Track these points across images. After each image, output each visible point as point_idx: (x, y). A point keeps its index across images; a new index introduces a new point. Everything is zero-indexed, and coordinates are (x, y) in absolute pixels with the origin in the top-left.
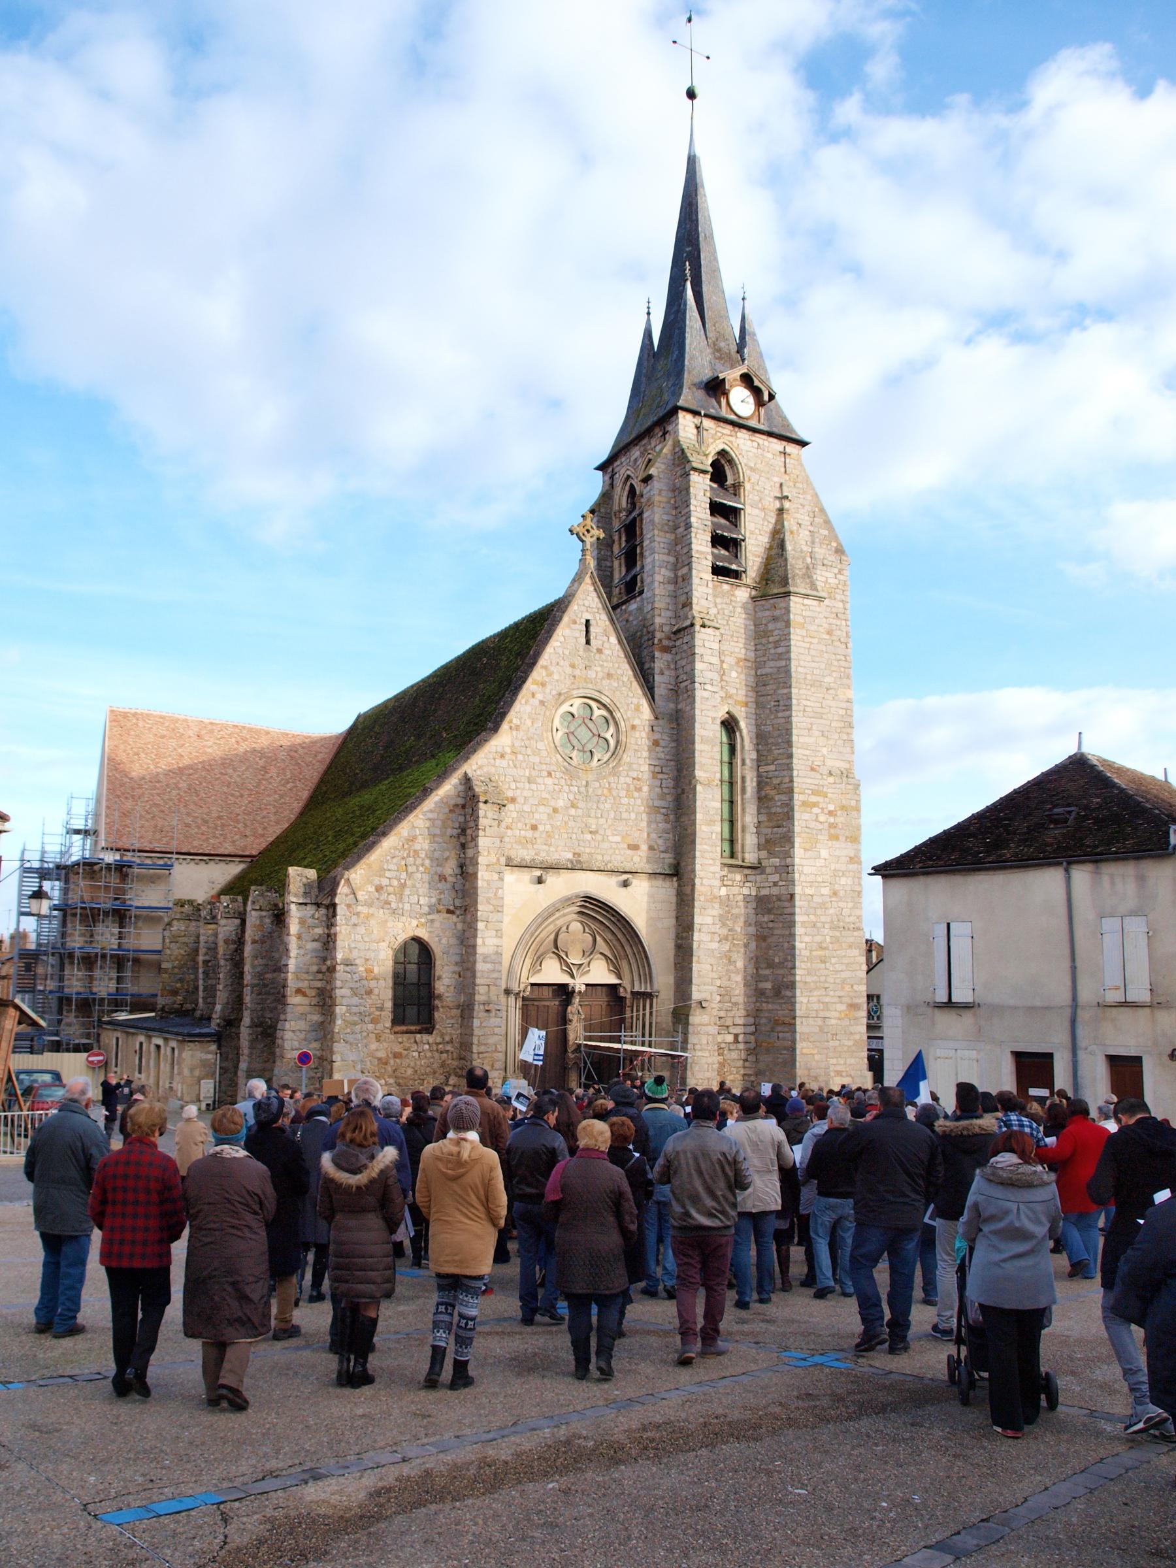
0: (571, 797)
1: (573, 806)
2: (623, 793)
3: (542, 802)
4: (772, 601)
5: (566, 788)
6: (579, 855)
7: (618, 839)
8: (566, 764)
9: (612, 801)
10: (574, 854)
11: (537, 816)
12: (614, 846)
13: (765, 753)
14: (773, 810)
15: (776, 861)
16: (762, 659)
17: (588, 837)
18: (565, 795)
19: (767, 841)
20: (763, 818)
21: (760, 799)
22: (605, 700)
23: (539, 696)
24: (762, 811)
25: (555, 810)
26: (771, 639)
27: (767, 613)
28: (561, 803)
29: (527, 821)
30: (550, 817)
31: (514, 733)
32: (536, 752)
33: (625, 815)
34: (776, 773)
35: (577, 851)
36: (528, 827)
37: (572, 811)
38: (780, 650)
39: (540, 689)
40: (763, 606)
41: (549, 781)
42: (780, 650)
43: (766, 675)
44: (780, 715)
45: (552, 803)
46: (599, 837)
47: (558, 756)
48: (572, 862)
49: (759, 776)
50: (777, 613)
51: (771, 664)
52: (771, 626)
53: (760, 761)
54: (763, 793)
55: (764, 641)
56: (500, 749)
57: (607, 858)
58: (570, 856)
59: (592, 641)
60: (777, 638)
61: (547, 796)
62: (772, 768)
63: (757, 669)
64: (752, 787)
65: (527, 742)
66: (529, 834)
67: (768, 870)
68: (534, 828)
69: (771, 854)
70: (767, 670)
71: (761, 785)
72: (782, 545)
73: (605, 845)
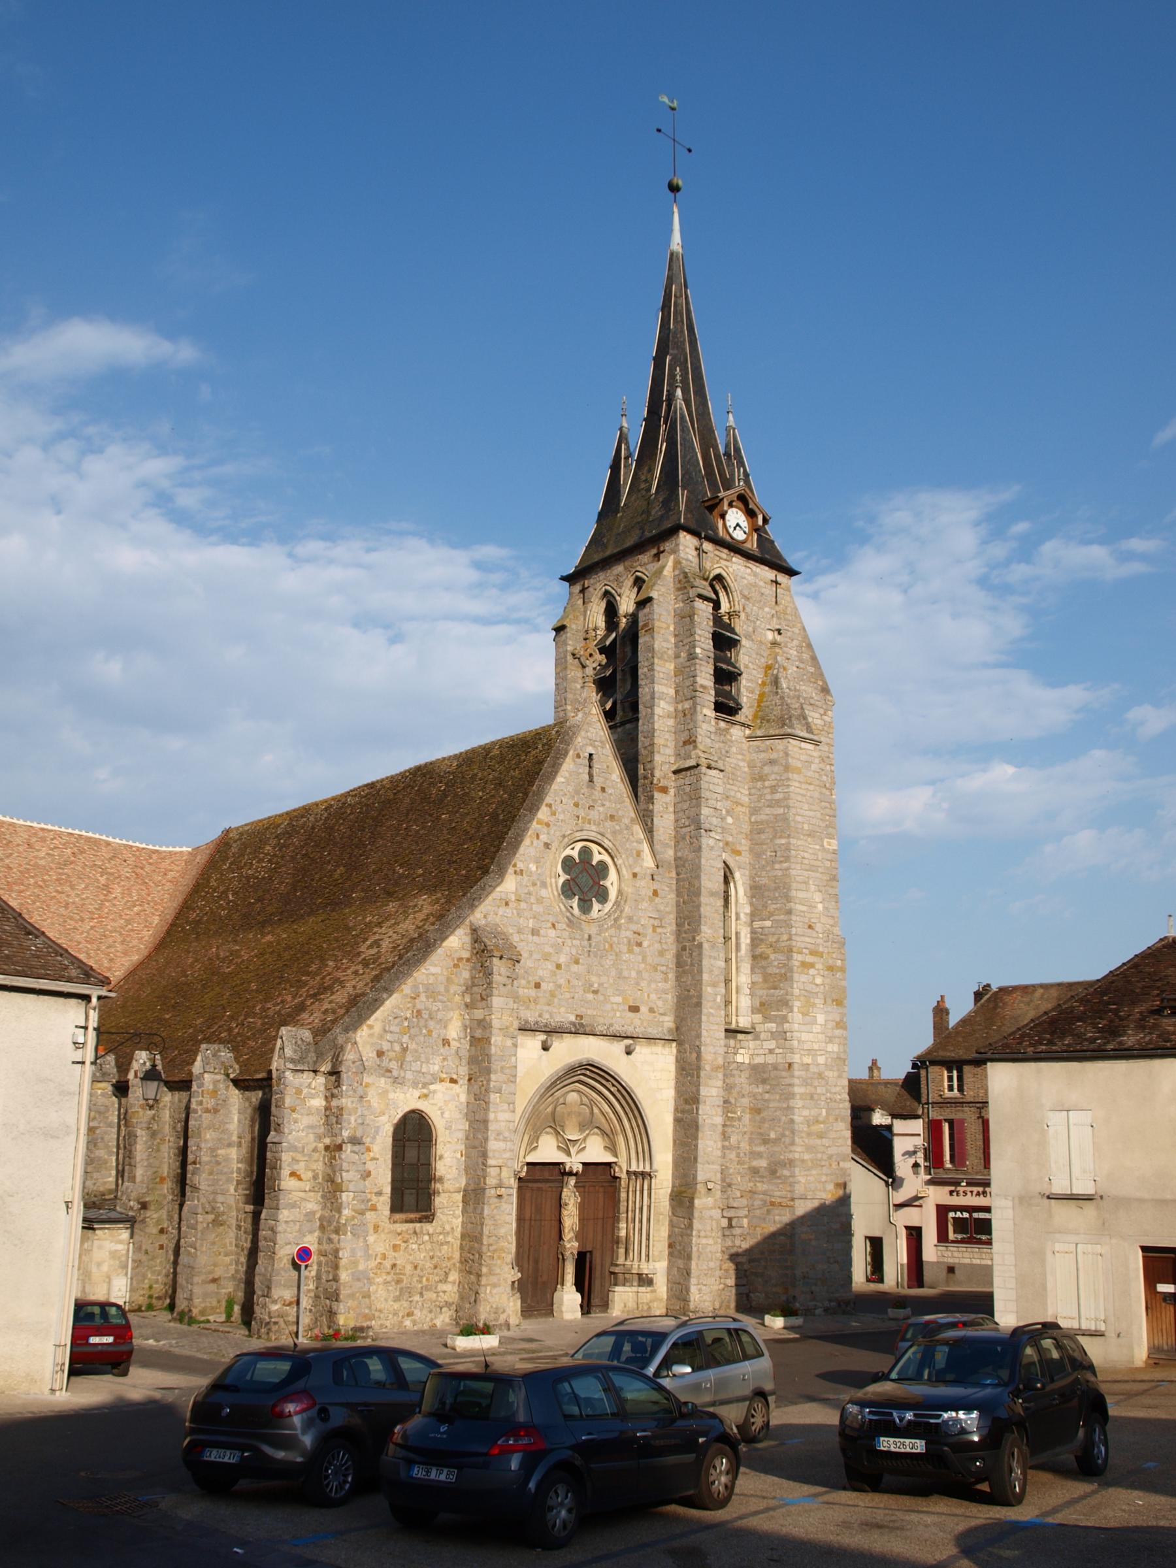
0: (574, 951)
1: (577, 962)
2: (624, 948)
3: (546, 957)
4: (768, 743)
5: (569, 942)
6: (581, 1017)
7: (619, 999)
8: (568, 914)
9: (614, 957)
10: (577, 1016)
11: (540, 973)
12: (615, 1007)
13: (760, 908)
14: (769, 970)
15: (772, 1026)
16: (756, 804)
17: (590, 996)
18: (568, 949)
19: (762, 1004)
20: (758, 978)
21: (754, 957)
22: (607, 843)
23: (544, 838)
24: (756, 970)
25: (558, 966)
26: (767, 784)
27: (763, 755)
28: (562, 959)
29: (530, 979)
30: (554, 974)
31: (519, 877)
32: (540, 900)
33: (625, 973)
34: (773, 930)
36: (533, 985)
37: (575, 968)
38: (778, 796)
39: (545, 830)
40: (758, 747)
41: (552, 933)
42: (778, 796)
43: (762, 823)
44: (777, 866)
45: (554, 959)
46: (601, 998)
47: (561, 905)
48: (574, 1024)
49: (753, 932)
50: (774, 756)
51: (768, 811)
52: (767, 769)
53: (754, 915)
54: (759, 951)
55: (759, 784)
56: (503, 896)
58: (572, 1018)
59: (595, 779)
60: (774, 783)
61: (551, 950)
62: (768, 923)
63: (752, 814)
64: (747, 944)
65: (531, 889)
66: (532, 992)
67: (763, 1036)
68: (538, 986)
69: (767, 1019)
70: (764, 817)
71: (755, 941)
72: (776, 682)
73: (608, 1007)
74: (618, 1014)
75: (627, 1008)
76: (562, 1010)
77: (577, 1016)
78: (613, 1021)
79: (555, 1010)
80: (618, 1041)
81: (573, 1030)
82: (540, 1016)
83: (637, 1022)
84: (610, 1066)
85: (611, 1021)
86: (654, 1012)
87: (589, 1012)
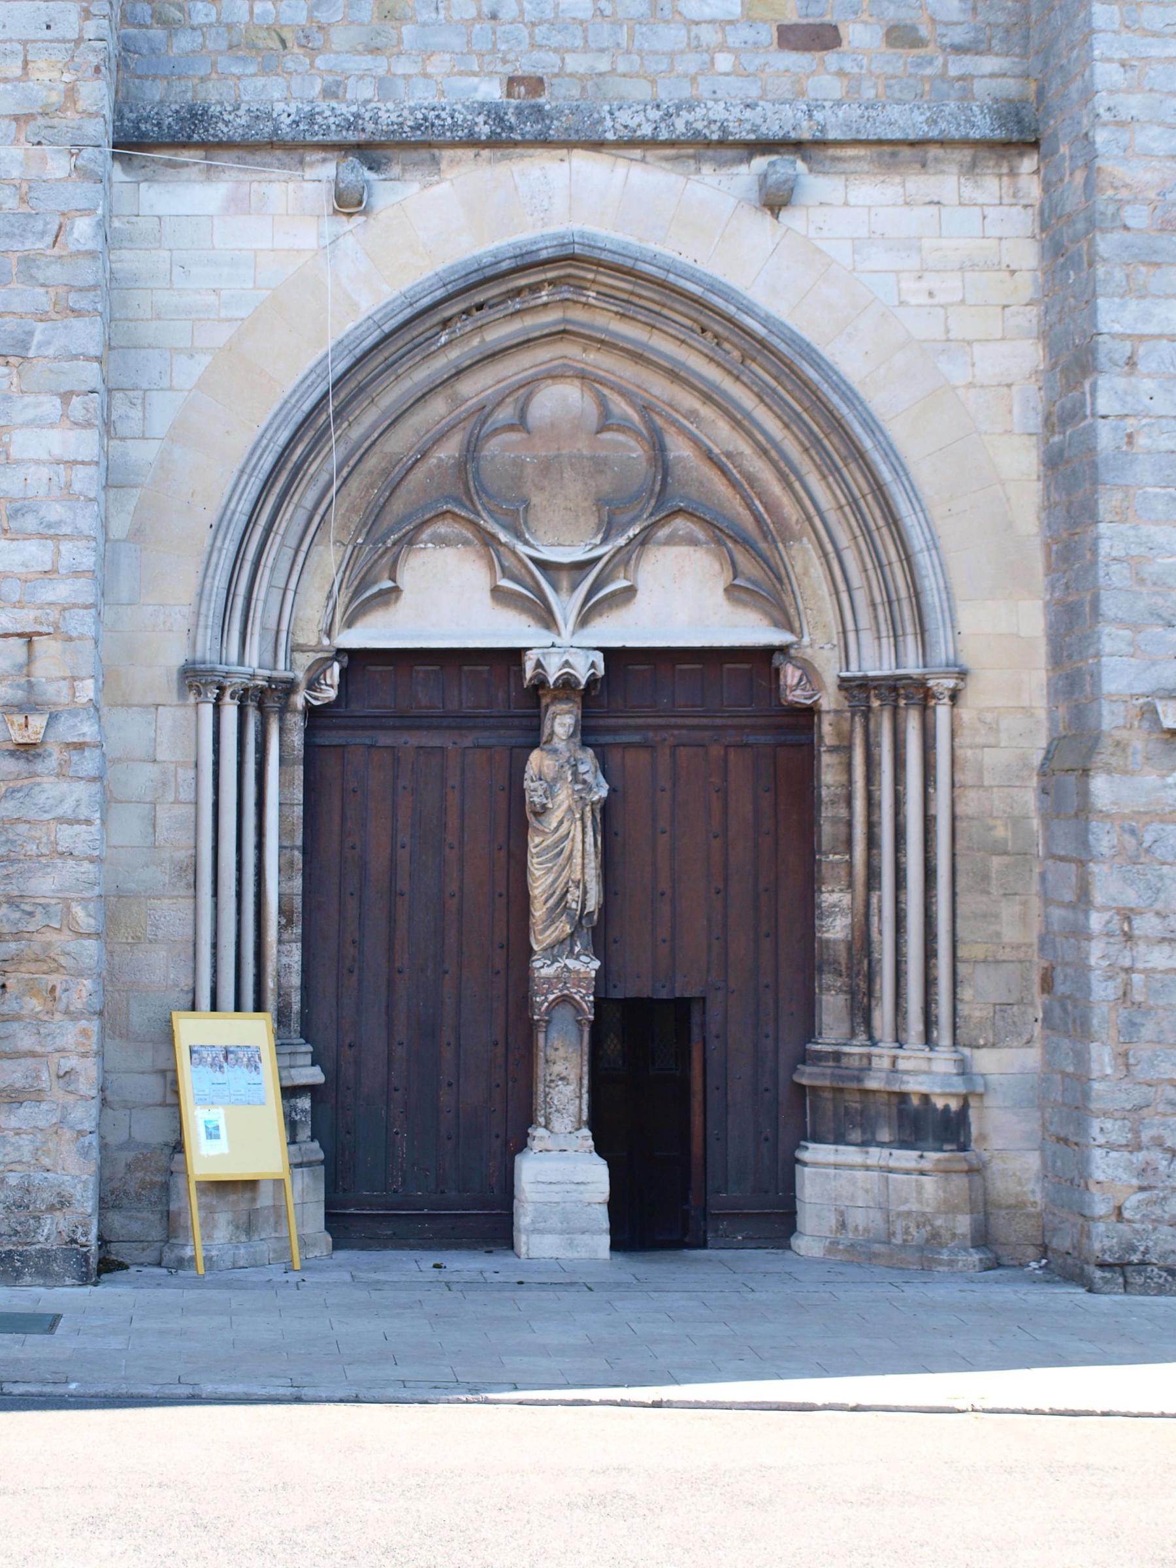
6: (536, 85)
10: (512, 81)
12: (708, 35)
35: (524, 68)
48: (495, 113)
57: (668, 93)
58: (492, 91)
74: (724, 62)
75: (768, 34)
76: (438, 66)
77: (512, 81)
78: (704, 88)
79: (403, 67)
80: (721, 164)
81: (483, 130)
82: (330, 93)
83: (827, 86)
84: (686, 259)
85: (686, 92)
86: (917, 42)
87: (574, 63)
